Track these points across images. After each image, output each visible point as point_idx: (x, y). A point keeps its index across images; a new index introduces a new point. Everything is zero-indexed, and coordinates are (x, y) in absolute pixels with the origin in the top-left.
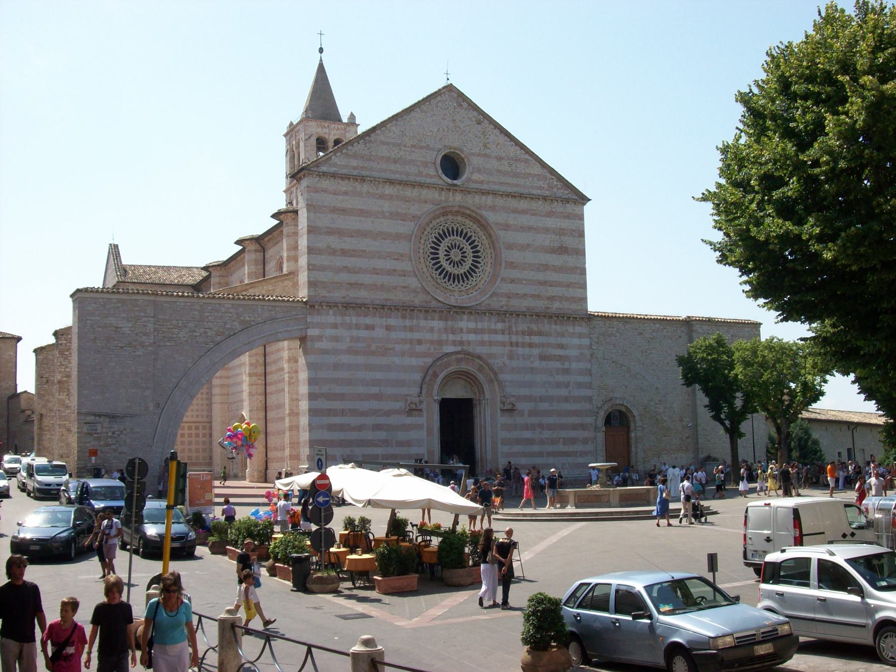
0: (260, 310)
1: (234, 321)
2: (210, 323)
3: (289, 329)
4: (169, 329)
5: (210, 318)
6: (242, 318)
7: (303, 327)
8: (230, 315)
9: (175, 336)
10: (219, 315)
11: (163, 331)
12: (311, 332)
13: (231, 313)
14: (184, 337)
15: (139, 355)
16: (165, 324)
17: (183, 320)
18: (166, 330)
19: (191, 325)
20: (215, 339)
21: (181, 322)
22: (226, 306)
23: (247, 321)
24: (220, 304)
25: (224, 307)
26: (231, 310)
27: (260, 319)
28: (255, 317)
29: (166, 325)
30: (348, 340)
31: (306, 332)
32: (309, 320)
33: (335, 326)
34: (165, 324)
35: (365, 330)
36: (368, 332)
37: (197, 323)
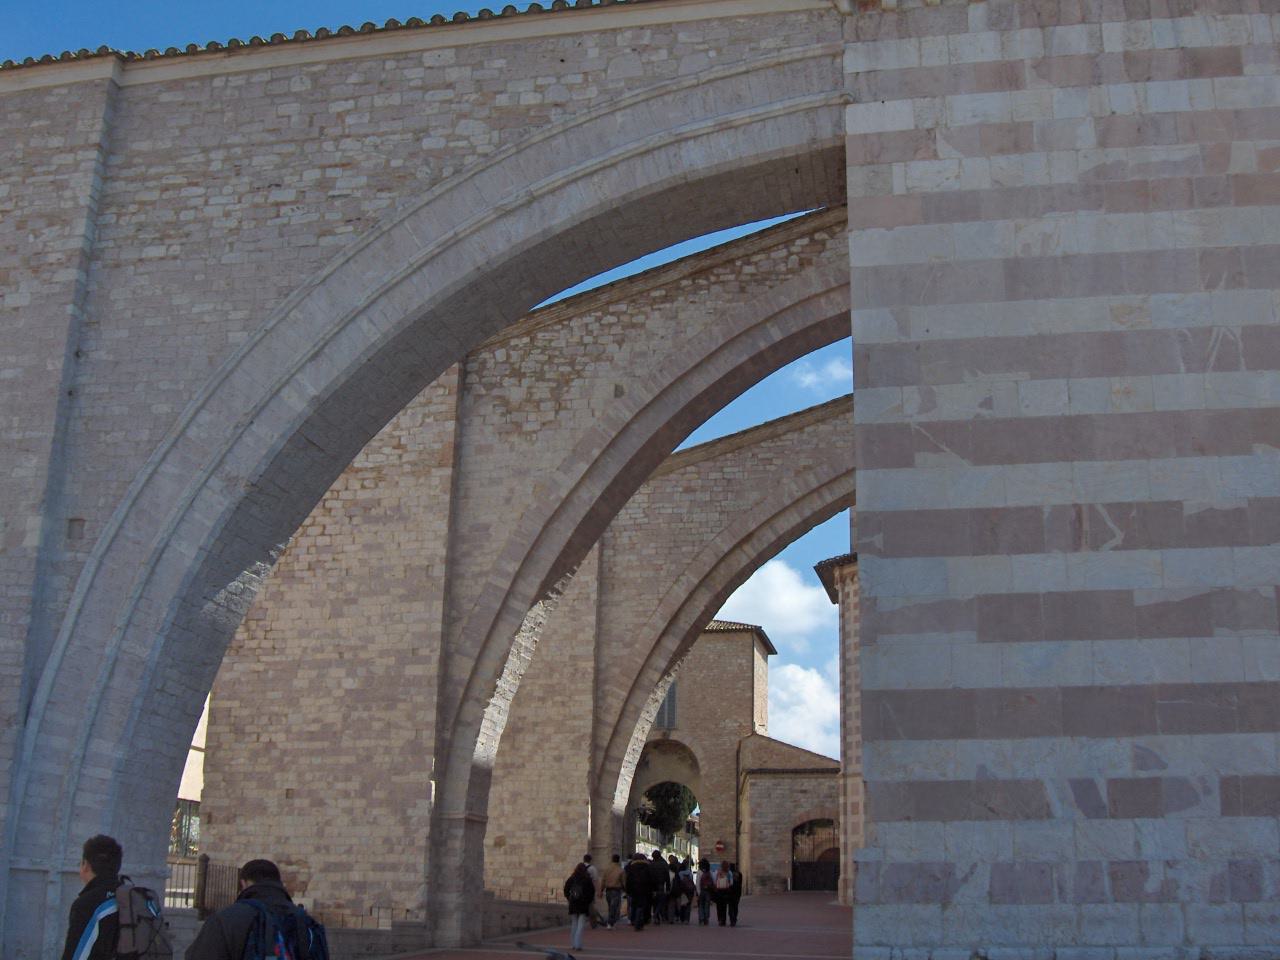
0: (593, 53)
1: (463, 116)
2: (347, 143)
3: (739, 116)
4: (166, 189)
5: (349, 120)
6: (502, 100)
7: (817, 99)
8: (449, 94)
9: (183, 216)
10: (395, 99)
11: (143, 203)
12: (860, 121)
13: (450, 86)
14: (227, 215)
15: (16, 309)
16: (152, 171)
17: (228, 147)
18: (155, 195)
19: (264, 161)
20: (366, 206)
21: (220, 154)
22: (429, 59)
23: (529, 108)
24: (401, 57)
25: (420, 64)
26: (453, 75)
27: (592, 92)
28: (570, 87)
29: (159, 177)
30: (1087, 135)
31: (839, 124)
32: (854, 61)
33: (1006, 77)
34: (152, 171)
35: (1181, 76)
36: (1202, 85)
37: (291, 148)
